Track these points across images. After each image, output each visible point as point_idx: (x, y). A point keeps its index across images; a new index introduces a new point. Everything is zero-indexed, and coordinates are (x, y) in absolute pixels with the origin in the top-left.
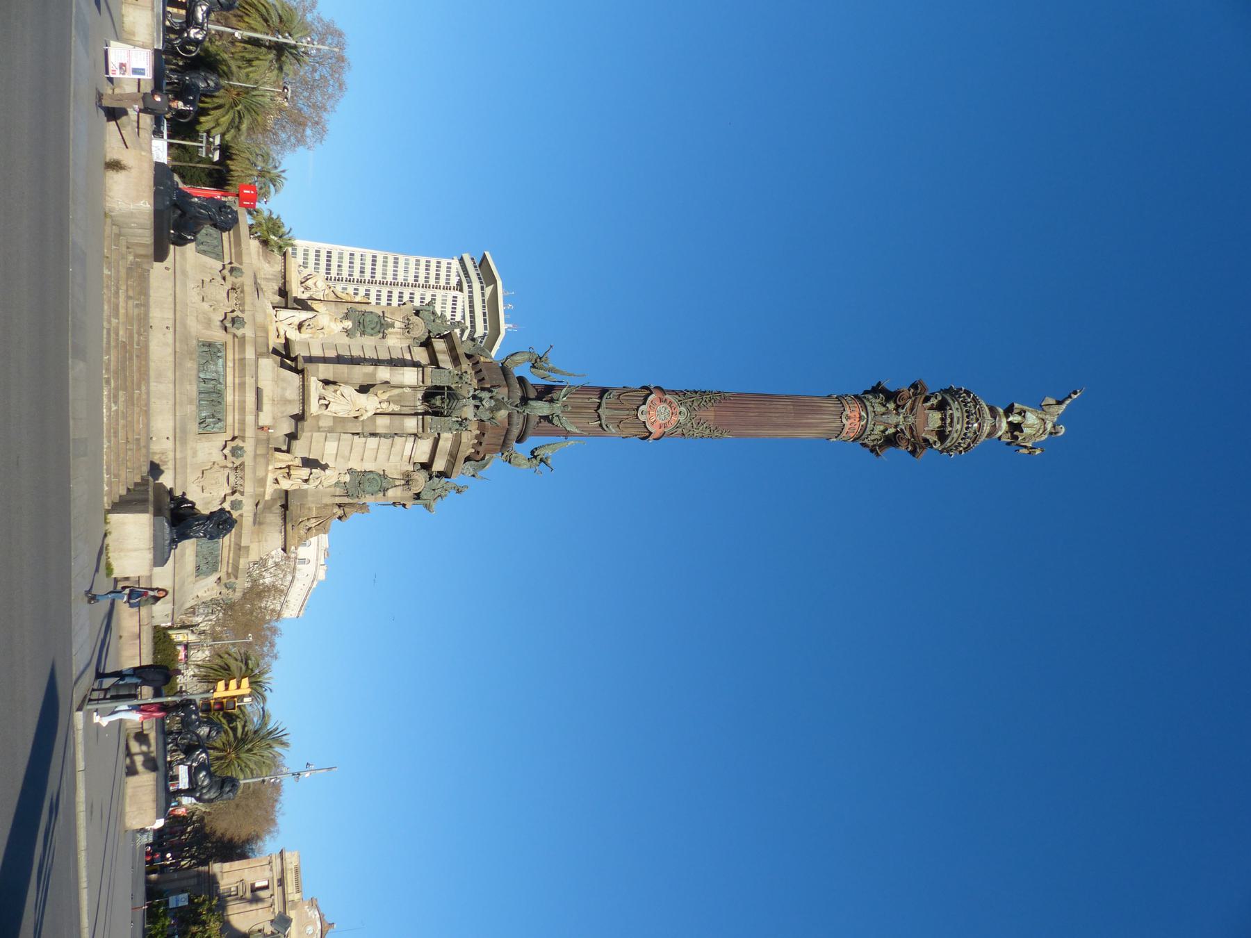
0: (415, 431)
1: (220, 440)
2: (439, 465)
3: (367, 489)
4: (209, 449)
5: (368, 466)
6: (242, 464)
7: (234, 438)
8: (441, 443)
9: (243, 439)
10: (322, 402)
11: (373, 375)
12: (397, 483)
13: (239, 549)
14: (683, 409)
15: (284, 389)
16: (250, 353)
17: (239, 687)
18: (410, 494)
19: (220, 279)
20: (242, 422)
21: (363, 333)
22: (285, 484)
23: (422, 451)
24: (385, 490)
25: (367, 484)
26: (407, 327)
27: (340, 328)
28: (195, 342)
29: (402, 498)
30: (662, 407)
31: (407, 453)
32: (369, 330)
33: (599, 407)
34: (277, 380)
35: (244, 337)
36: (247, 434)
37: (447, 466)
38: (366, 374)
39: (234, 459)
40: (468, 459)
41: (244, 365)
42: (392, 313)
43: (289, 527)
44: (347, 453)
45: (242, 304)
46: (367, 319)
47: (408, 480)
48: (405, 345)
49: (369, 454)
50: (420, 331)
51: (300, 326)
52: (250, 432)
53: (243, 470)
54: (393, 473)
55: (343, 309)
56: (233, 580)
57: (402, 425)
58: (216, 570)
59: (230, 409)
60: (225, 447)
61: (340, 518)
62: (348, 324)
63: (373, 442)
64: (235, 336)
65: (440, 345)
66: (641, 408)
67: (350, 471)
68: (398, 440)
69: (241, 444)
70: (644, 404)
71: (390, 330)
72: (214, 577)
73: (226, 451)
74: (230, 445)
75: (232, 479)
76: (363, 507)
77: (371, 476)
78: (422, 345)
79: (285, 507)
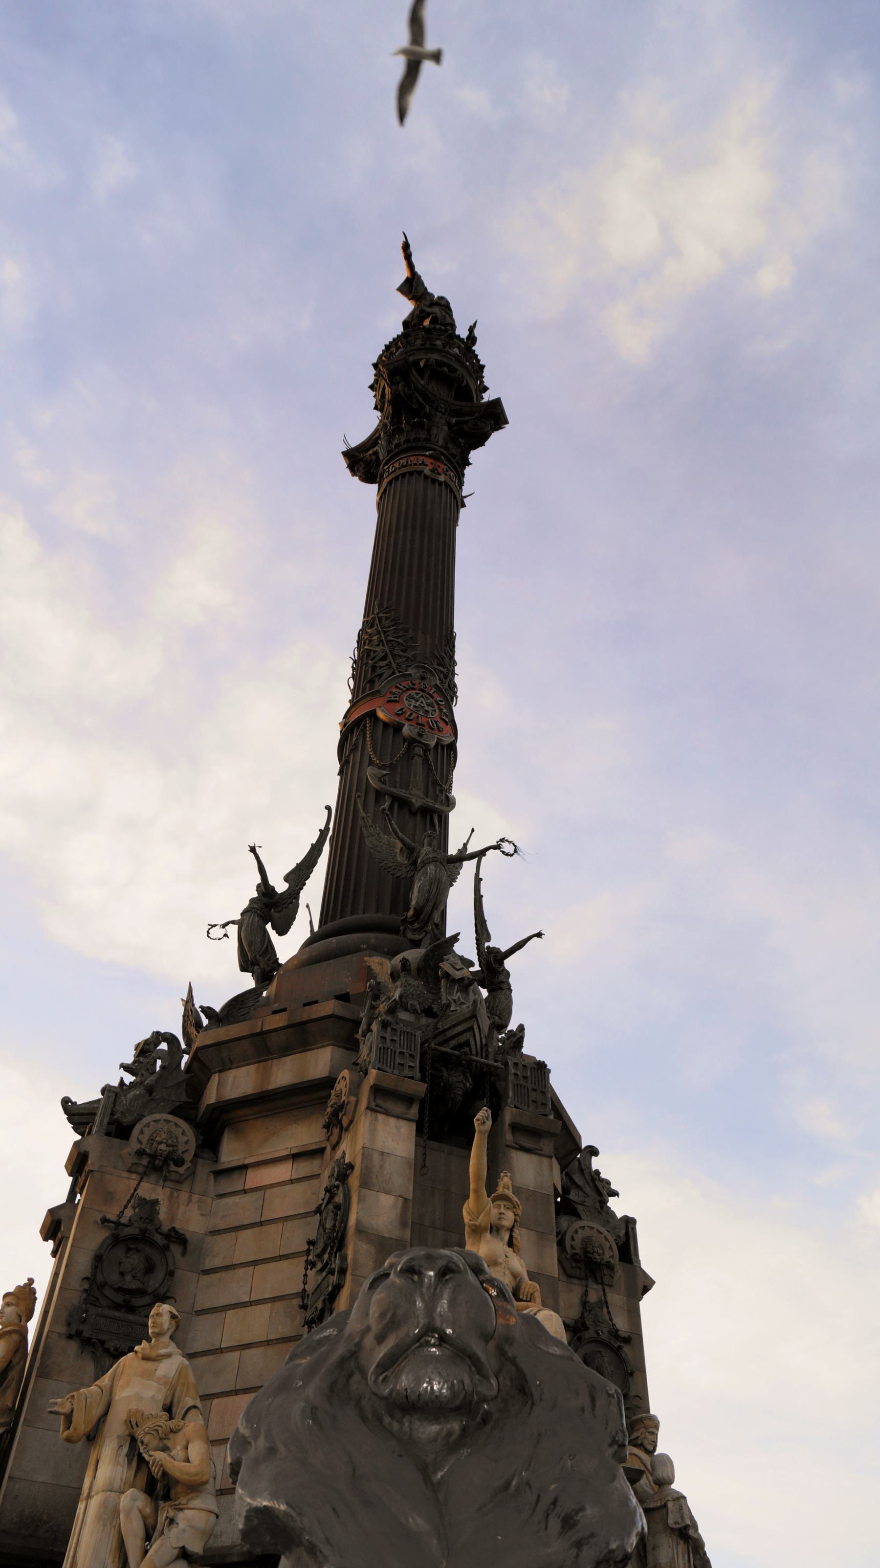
12: (593, 1297)
18: (620, 1270)
42: (109, 1197)
46: (114, 1278)
71: (163, 1213)
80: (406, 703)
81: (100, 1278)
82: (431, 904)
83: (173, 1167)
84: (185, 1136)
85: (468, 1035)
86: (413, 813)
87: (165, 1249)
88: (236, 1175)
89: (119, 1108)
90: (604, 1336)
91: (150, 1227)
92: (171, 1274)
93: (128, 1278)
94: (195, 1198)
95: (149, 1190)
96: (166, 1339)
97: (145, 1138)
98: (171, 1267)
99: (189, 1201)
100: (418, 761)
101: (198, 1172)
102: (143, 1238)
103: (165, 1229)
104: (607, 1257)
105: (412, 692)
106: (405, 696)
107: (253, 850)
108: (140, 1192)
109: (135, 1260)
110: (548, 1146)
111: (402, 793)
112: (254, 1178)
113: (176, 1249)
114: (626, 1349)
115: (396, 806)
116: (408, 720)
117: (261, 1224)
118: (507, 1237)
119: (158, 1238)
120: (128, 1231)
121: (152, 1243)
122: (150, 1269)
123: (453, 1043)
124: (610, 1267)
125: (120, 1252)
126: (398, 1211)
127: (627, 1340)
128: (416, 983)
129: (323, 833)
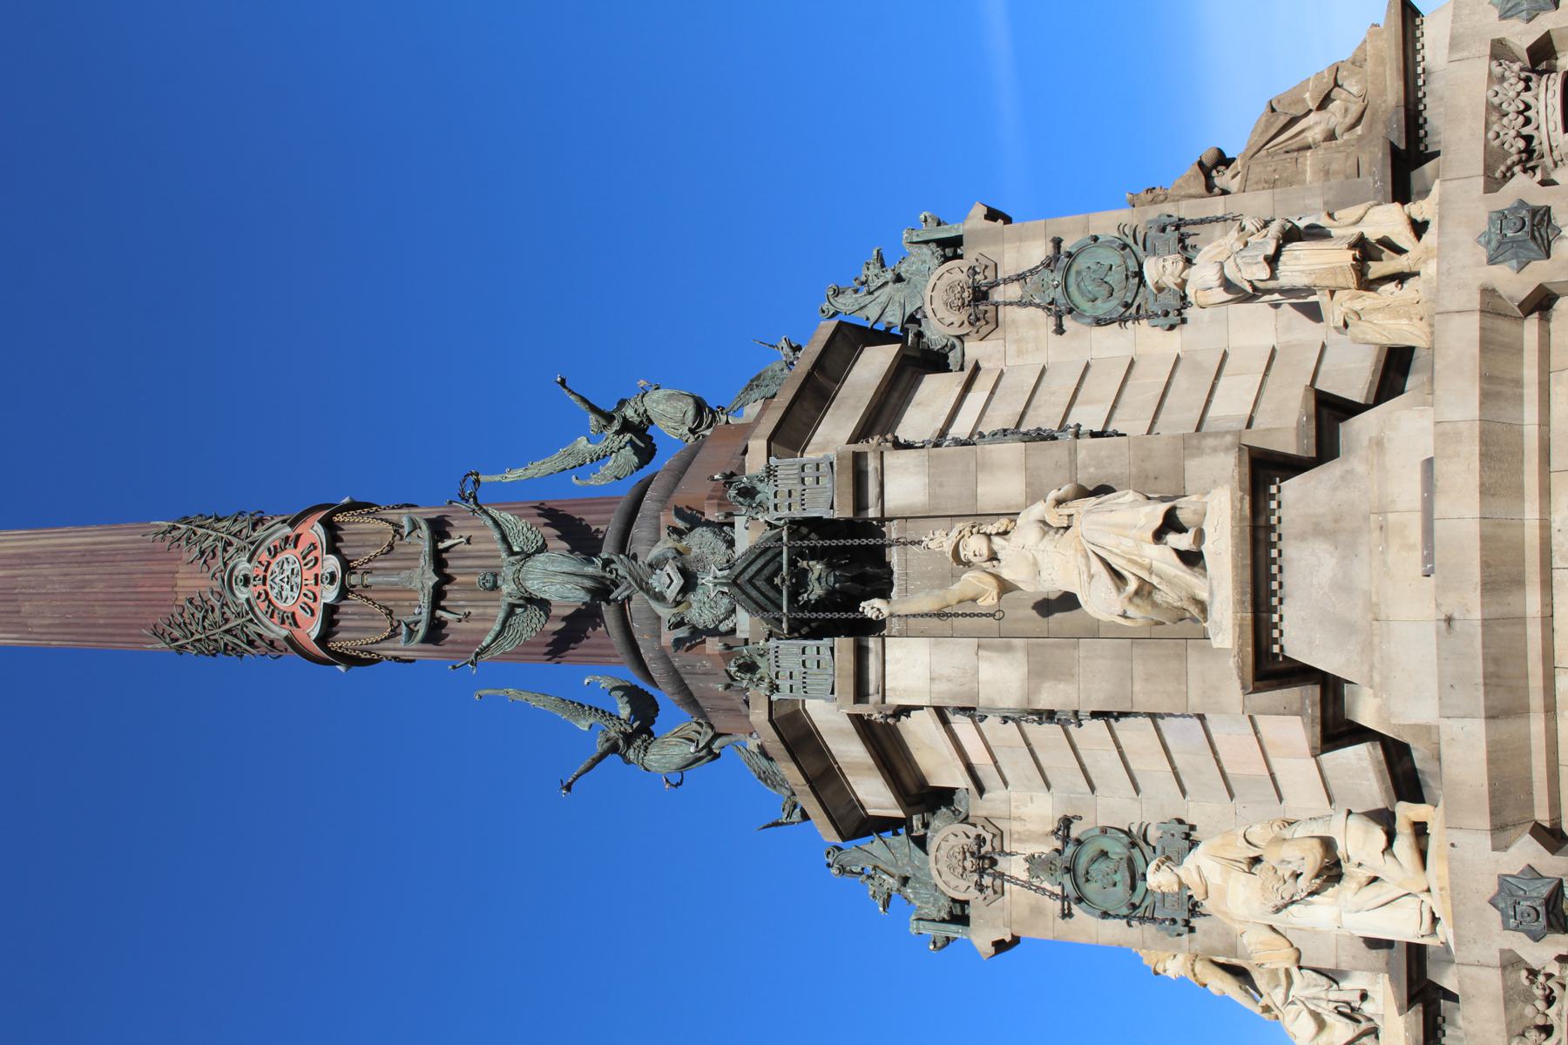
3: (1113, 258)
5: (1112, 344)
6: (1493, 183)
9: (1491, 304)
10: (1184, 542)
11: (1038, 673)
12: (1014, 291)
14: (242, 594)
15: (1343, 586)
18: (970, 254)
22: (1387, 221)
24: (1050, 263)
25: (1115, 278)
26: (984, 861)
29: (997, 239)
30: (288, 602)
32: (1117, 849)
33: (438, 595)
34: (1370, 626)
35: (1500, 829)
36: (1474, 321)
38: (1064, 673)
41: (1492, 680)
43: (1393, 92)
45: (1511, 997)
48: (995, 793)
51: (1331, 871)
53: (1492, 158)
57: (934, 482)
61: (1223, 161)
65: (875, 795)
70: (330, 610)
78: (944, 797)
80: (290, 602)
81: (1125, 911)
82: (579, 580)
83: (987, 848)
84: (947, 836)
85: (759, 583)
87: (1079, 842)
88: (980, 774)
89: (935, 915)
91: (1058, 862)
92: (1104, 831)
93: (1117, 877)
94: (1015, 812)
95: (1015, 867)
96: (1180, 871)
97: (963, 884)
98: (1097, 832)
99: (1020, 819)
100: (368, 580)
101: (985, 813)
103: (1058, 844)
104: (963, 277)
105: (272, 595)
106: (279, 604)
107: (568, 788)
108: (1024, 876)
111: (424, 600)
112: (978, 756)
114: (1066, 246)
115: (443, 603)
116: (315, 599)
117: (1028, 744)
118: (997, 540)
119: (1069, 851)
120: (1069, 888)
121: (1075, 857)
123: (772, 594)
125: (1090, 889)
126: (995, 655)
127: (1057, 243)
128: (695, 605)
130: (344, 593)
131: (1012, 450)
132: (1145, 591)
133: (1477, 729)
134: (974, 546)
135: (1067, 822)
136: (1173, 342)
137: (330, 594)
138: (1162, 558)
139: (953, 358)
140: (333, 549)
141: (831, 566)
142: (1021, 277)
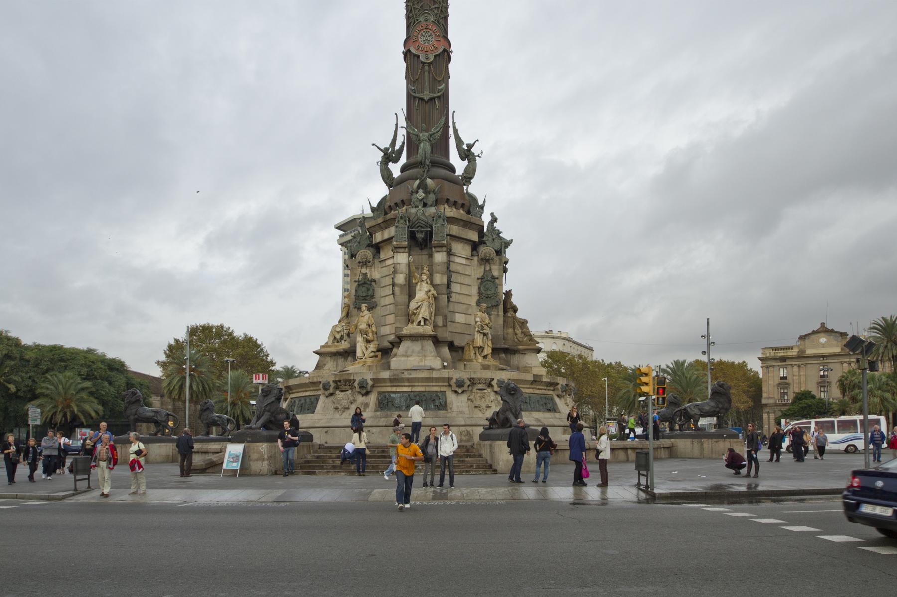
0: (445, 253)
1: (450, 396)
2: (474, 236)
4: (458, 403)
5: (474, 290)
7: (450, 385)
8: (454, 233)
9: (450, 379)
10: (422, 323)
11: (401, 286)
12: (488, 268)
13: (536, 380)
14: (421, 19)
16: (385, 375)
17: (647, 384)
18: (497, 259)
19: (332, 398)
20: (437, 380)
21: (372, 296)
22: (488, 351)
23: (461, 250)
24: (493, 277)
25: (489, 292)
26: (365, 263)
27: (366, 312)
28: (378, 413)
29: (500, 264)
31: (464, 261)
32: (370, 292)
33: (422, 99)
35: (373, 380)
37: (473, 229)
39: (466, 386)
40: (469, 212)
42: (356, 275)
44: (465, 307)
46: (361, 294)
47: (485, 261)
49: (465, 290)
50: (369, 253)
52: (445, 374)
54: (479, 272)
55: (354, 312)
56: (559, 386)
57: (438, 264)
58: (552, 399)
59: (428, 389)
60: (456, 392)
62: (364, 307)
63: (456, 287)
64: (373, 386)
65: (378, 237)
66: (422, 59)
67: (478, 304)
68: (453, 267)
69: (454, 380)
70: (418, 57)
72: (557, 400)
73: (460, 391)
74: (455, 388)
75: (481, 387)
76: (508, 294)
77: (482, 289)
79: (506, 351)
86: (427, 102)
90: (489, 278)
95: (364, 270)
100: (426, 73)
102: (365, 283)
109: (364, 289)
110: (444, 249)
111: (421, 95)
113: (373, 283)
114: (497, 280)
122: (368, 290)
124: (493, 259)
129: (397, 125)
130: (424, 63)
131: (445, 281)
132: (414, 314)
133: (387, 377)
134: (424, 277)
135: (375, 281)
136: (474, 304)
137: (422, 59)
138: (420, 318)
139: (475, 252)
140: (435, 56)
141: (423, 239)
142: (490, 270)
